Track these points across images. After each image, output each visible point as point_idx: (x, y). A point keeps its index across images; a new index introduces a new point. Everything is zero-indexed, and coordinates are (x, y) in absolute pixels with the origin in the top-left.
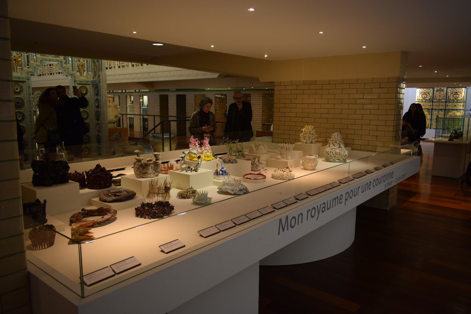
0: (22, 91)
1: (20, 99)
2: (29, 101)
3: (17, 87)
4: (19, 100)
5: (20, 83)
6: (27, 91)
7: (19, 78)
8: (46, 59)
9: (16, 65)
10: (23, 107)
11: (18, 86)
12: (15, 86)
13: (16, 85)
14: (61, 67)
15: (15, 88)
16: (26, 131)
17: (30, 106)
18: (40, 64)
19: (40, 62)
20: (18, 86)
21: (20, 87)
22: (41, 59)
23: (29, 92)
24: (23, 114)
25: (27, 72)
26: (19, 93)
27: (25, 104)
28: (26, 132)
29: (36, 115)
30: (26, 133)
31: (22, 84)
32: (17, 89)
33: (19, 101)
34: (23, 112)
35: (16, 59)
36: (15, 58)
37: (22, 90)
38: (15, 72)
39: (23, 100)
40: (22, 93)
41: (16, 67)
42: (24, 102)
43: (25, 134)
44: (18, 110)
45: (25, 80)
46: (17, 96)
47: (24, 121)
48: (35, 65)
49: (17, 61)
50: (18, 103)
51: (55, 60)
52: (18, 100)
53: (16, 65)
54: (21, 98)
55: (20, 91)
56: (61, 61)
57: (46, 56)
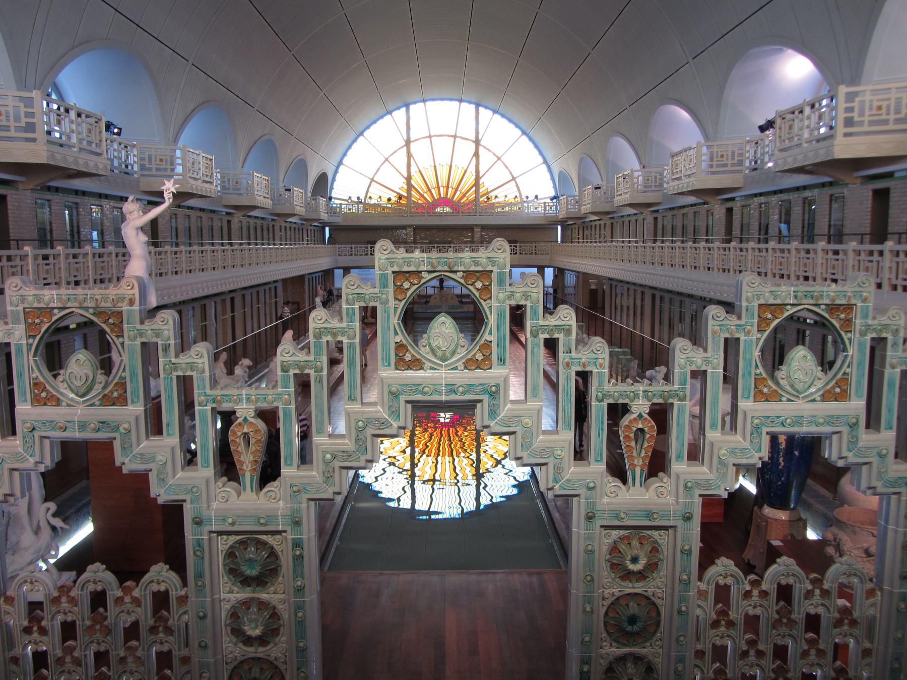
0: (656, 564)
1: (644, 602)
2: (680, 612)
6: (678, 569)
8: (778, 417)
13: (635, 543)
14: (849, 450)
17: (682, 639)
18: (747, 444)
19: (752, 434)
21: (648, 548)
22: (756, 421)
23: (685, 577)
24: (649, 662)
25: (686, 486)
26: (641, 576)
27: (662, 623)
29: (705, 671)
32: (635, 560)
34: (650, 657)
35: (646, 429)
36: (640, 426)
38: (634, 485)
42: (659, 614)
44: (631, 647)
45: (671, 523)
48: (723, 451)
49: (648, 436)
51: (821, 420)
52: (633, 609)
56: (854, 420)
57: (781, 401)
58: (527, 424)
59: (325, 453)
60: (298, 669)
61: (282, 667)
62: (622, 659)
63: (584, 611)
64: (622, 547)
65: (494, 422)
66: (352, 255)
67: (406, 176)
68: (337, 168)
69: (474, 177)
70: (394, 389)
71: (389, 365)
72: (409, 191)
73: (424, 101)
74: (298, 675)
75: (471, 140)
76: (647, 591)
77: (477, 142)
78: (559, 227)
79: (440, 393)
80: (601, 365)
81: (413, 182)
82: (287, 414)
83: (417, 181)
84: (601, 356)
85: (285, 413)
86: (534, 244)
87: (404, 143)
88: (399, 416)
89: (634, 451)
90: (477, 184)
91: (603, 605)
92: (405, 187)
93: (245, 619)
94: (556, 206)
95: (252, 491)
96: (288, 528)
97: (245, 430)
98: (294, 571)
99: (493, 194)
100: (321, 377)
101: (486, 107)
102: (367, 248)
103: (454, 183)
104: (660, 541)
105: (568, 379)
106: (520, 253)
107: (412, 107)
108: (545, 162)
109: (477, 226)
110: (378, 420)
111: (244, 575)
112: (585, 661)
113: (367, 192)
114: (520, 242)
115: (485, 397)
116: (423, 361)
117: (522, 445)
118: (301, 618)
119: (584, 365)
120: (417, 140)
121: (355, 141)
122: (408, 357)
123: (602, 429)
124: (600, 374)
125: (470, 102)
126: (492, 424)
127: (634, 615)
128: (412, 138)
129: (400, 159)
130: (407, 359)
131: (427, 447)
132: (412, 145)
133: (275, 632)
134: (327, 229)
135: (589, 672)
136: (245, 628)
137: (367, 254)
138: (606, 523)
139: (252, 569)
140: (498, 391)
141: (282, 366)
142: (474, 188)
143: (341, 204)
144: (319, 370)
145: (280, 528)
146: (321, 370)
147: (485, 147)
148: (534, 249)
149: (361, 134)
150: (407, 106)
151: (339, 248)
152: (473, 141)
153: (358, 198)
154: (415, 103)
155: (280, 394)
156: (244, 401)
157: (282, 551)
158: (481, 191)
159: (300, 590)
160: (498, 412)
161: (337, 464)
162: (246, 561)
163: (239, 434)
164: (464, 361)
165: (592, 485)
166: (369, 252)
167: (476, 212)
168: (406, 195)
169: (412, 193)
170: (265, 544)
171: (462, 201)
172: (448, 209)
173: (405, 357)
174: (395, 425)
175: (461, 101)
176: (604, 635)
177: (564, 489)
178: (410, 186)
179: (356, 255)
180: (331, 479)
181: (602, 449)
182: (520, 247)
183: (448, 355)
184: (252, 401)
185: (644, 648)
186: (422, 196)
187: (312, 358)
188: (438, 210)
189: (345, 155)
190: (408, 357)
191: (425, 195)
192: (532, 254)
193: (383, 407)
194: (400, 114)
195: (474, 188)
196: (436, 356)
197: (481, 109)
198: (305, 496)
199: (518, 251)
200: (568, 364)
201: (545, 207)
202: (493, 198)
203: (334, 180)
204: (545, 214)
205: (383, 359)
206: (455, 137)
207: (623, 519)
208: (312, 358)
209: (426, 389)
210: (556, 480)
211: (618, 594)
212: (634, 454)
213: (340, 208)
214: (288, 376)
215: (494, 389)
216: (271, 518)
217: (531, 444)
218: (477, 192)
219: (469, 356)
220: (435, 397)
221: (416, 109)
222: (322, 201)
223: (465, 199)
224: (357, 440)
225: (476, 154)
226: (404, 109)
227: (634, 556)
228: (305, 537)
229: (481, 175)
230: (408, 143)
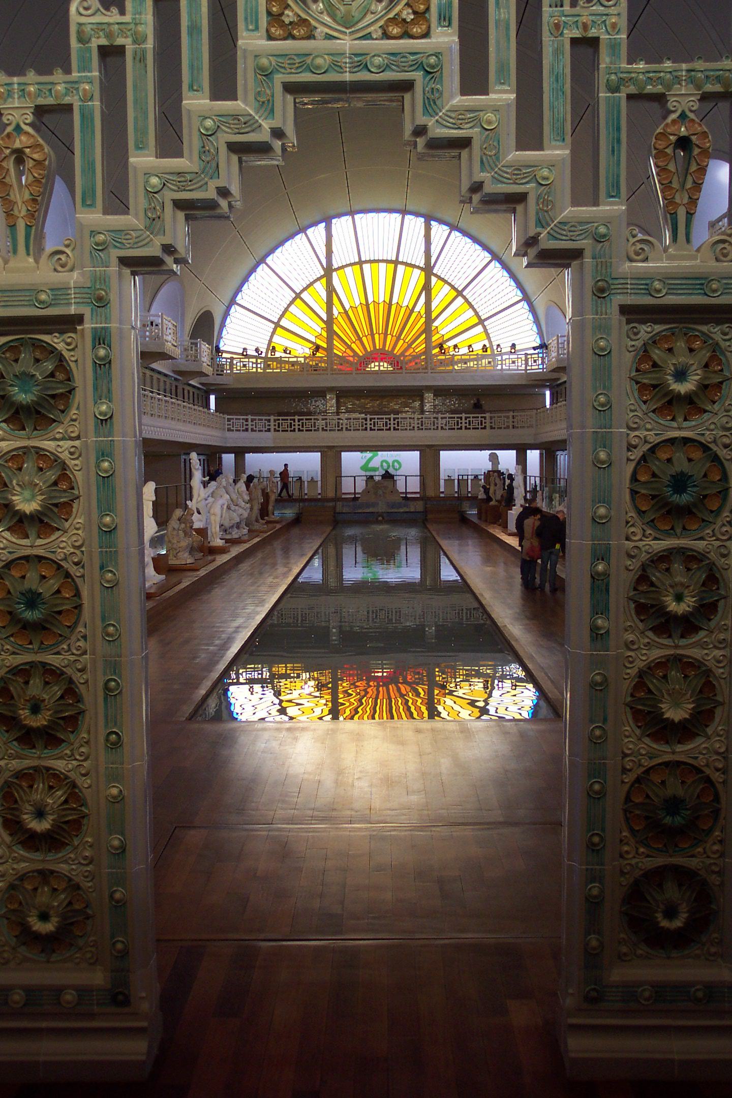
1: (697, 455)
3: (682, 358)
4: (690, 460)
5: (704, 328)
7: (701, 281)
9: (689, 185)
10: (717, 513)
11: (691, 350)
12: (670, 350)
15: (670, 364)
16: (722, 704)
20: (691, 350)
21: (705, 355)
28: (718, 712)
30: (717, 720)
31: (718, 337)
32: (681, 375)
33: (685, 467)
34: (712, 556)
35: (694, 138)
37: (717, 379)
39: (716, 458)
40: (716, 407)
41: (686, 200)
43: (709, 731)
46: (680, 429)
47: (712, 624)
49: (696, 151)
50: (680, 482)
52: (681, 463)
53: (689, 185)
54: (705, 448)
55: (704, 387)
58: (489, 122)
59: (148, 174)
60: (102, 567)
61: (74, 571)
62: (663, 558)
63: (597, 462)
64: (657, 354)
65: (434, 120)
66: (247, 430)
67: (325, 319)
68: (229, 308)
69: (423, 320)
70: (264, 61)
71: (257, 28)
72: (329, 340)
73: (352, 213)
74: (102, 577)
75: (418, 267)
76: (703, 435)
77: (428, 270)
78: (548, 393)
79: (339, 68)
80: (614, 25)
81: (335, 328)
82: (87, 117)
83: (341, 327)
84: (613, 11)
85: (83, 116)
86: (511, 414)
87: (323, 273)
88: (272, 111)
89: (675, 179)
90: (428, 329)
91: (628, 460)
92: (325, 334)
93: (14, 482)
94: (543, 358)
95: (28, 254)
96: (86, 311)
97: (17, 145)
98: (96, 388)
99: (451, 344)
100: (144, 51)
101: (441, 222)
102: (269, 421)
103: (395, 328)
104: (723, 344)
105: (557, 52)
106: (492, 428)
107: (334, 221)
108: (526, 298)
109: (428, 388)
110: (235, 117)
111: (13, 404)
112: (601, 554)
113: (270, 341)
114: (491, 412)
115: (417, 76)
116: (313, 23)
117: (482, 162)
118: (106, 471)
119: (585, 27)
120: (343, 267)
121: (253, 270)
122: (289, 16)
123: (619, 141)
124: (614, 47)
125: (417, 214)
126: (431, 123)
127: (682, 472)
128: (335, 266)
129: (317, 296)
130: (287, 21)
131: (357, 712)
132: (334, 274)
133: (66, 507)
134: (212, 398)
135: (606, 575)
136: (14, 498)
137: (269, 430)
138: (630, 300)
139: (26, 392)
140: (439, 66)
141: (79, 32)
142: (424, 336)
143: (232, 359)
144: (139, 39)
145: (73, 310)
146: (145, 40)
147: (439, 277)
148: (511, 420)
149: (262, 260)
150: (328, 221)
151: (229, 420)
152: (421, 269)
153: (257, 350)
154: (339, 216)
155: (76, 82)
156: (16, 96)
157: (76, 361)
158: (434, 339)
159: (105, 421)
160: (438, 102)
161: (169, 195)
162: (16, 376)
163: (8, 151)
164: (381, 23)
165: (602, 230)
166: (272, 428)
167: (426, 368)
168: (325, 345)
169: (335, 342)
170: (51, 351)
171: (407, 354)
172: (385, 366)
173: (283, 18)
174: (266, 125)
175: (404, 212)
176: (632, 514)
177: (557, 239)
178: (331, 334)
179: (252, 430)
180: (158, 223)
181: (618, 176)
182: (491, 418)
183: (357, 15)
184: (29, 94)
185: (702, 539)
186: (349, 347)
187: (127, 18)
188: (374, 367)
189: (239, 290)
190: (289, 16)
191: (354, 346)
192: (508, 427)
193: (245, 101)
194: (317, 233)
195: (424, 336)
196: (333, 17)
197: (432, 223)
198: (115, 253)
199: (488, 425)
200: (557, 26)
201: (526, 360)
202: (452, 349)
203: (223, 325)
204: (526, 370)
205: (246, 19)
206: (396, 262)
207: (659, 291)
208: (127, 18)
209: (319, 61)
210: (540, 223)
211: (654, 439)
212: (675, 185)
213: (231, 364)
214: (89, 50)
215: (432, 60)
216: (59, 293)
217: (498, 159)
218: (428, 340)
219: (391, 15)
220: (332, 77)
221: (341, 225)
222: (205, 347)
223: (412, 350)
224: (203, 151)
225: (427, 288)
226: (323, 224)
227: (679, 367)
228: (114, 325)
229: (434, 315)
230: (329, 271)
